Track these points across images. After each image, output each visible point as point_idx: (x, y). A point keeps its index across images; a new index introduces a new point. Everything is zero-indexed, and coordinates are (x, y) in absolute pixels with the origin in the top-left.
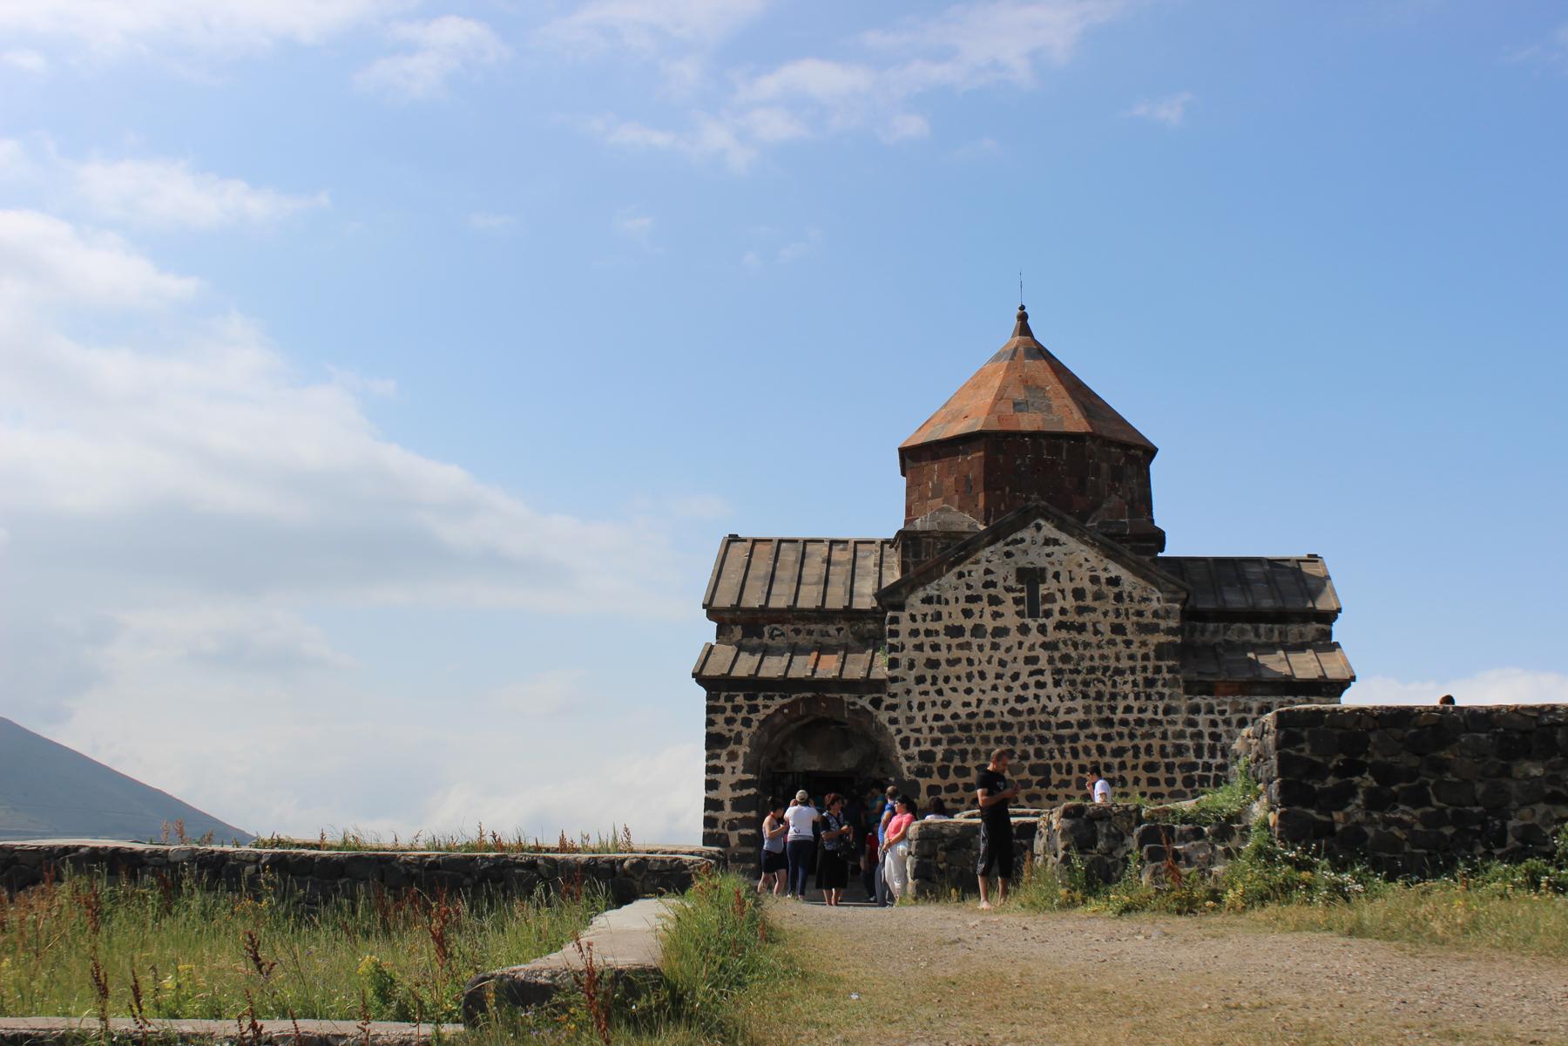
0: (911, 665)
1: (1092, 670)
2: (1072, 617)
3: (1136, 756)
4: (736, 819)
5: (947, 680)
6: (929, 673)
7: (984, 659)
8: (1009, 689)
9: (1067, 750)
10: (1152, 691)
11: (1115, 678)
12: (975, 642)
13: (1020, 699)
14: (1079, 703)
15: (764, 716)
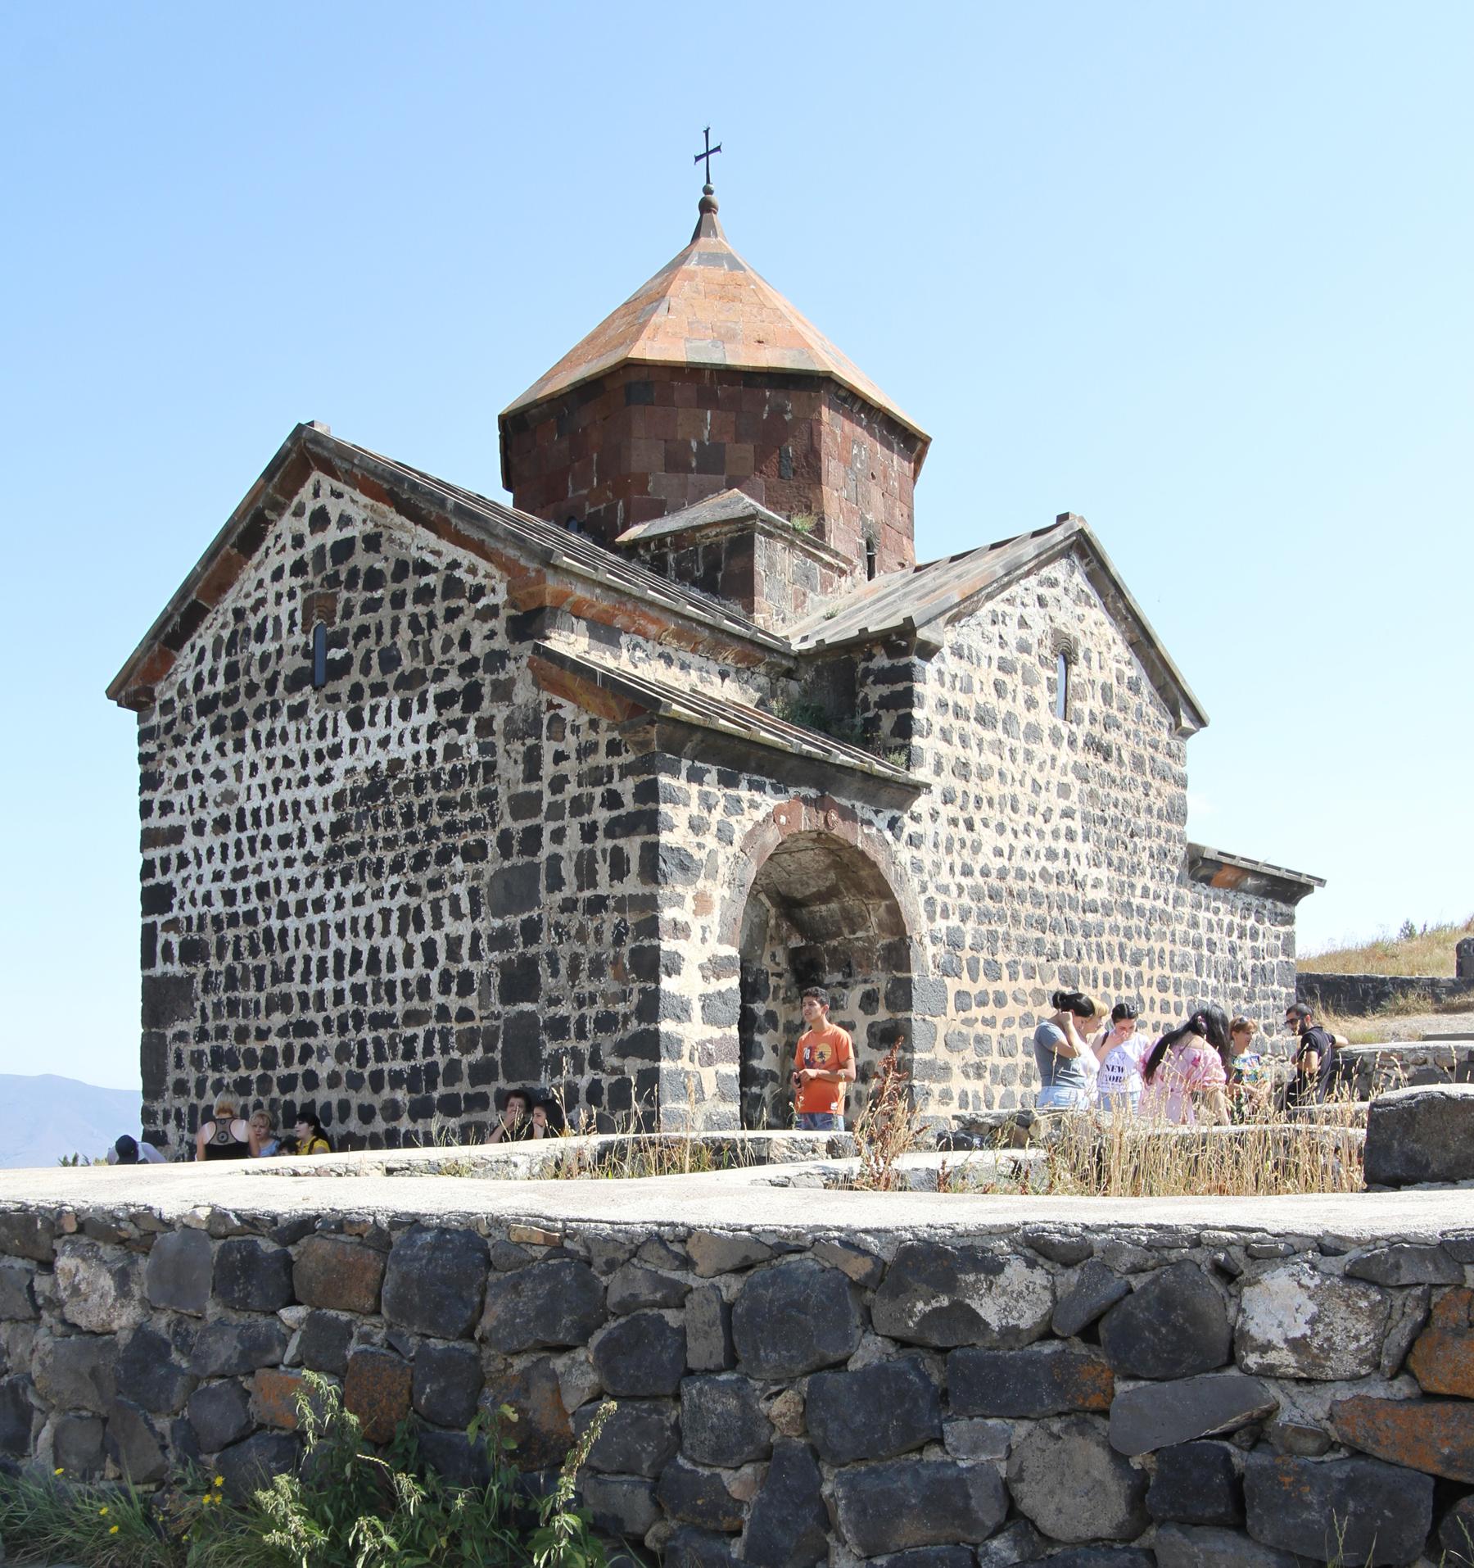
0: (938, 769)
1: (1115, 820)
2: (1097, 731)
3: (1151, 967)
4: (710, 1041)
5: (978, 801)
6: (959, 785)
7: (1018, 777)
8: (1040, 834)
9: (1094, 947)
10: (1164, 867)
11: (1136, 839)
12: (1009, 742)
13: (1052, 855)
14: (1104, 873)
15: (749, 826)
